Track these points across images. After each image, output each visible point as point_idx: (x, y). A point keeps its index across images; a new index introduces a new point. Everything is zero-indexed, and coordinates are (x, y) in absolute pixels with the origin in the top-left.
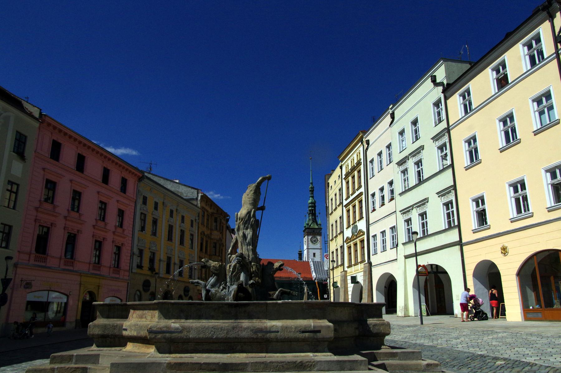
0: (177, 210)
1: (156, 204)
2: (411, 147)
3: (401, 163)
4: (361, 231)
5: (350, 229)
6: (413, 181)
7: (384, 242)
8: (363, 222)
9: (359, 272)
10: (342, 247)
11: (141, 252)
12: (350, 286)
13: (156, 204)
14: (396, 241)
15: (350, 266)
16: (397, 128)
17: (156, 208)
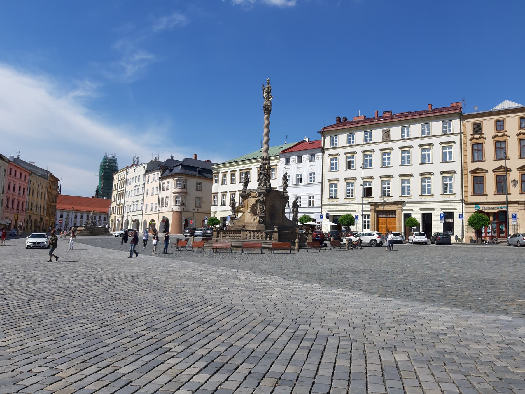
1: (34, 182)
2: (137, 184)
3: (135, 186)
4: (122, 203)
5: (119, 201)
8: (123, 200)
9: (119, 217)
10: (116, 207)
11: (28, 203)
12: (117, 222)
13: (34, 182)
15: (117, 215)
17: (34, 185)
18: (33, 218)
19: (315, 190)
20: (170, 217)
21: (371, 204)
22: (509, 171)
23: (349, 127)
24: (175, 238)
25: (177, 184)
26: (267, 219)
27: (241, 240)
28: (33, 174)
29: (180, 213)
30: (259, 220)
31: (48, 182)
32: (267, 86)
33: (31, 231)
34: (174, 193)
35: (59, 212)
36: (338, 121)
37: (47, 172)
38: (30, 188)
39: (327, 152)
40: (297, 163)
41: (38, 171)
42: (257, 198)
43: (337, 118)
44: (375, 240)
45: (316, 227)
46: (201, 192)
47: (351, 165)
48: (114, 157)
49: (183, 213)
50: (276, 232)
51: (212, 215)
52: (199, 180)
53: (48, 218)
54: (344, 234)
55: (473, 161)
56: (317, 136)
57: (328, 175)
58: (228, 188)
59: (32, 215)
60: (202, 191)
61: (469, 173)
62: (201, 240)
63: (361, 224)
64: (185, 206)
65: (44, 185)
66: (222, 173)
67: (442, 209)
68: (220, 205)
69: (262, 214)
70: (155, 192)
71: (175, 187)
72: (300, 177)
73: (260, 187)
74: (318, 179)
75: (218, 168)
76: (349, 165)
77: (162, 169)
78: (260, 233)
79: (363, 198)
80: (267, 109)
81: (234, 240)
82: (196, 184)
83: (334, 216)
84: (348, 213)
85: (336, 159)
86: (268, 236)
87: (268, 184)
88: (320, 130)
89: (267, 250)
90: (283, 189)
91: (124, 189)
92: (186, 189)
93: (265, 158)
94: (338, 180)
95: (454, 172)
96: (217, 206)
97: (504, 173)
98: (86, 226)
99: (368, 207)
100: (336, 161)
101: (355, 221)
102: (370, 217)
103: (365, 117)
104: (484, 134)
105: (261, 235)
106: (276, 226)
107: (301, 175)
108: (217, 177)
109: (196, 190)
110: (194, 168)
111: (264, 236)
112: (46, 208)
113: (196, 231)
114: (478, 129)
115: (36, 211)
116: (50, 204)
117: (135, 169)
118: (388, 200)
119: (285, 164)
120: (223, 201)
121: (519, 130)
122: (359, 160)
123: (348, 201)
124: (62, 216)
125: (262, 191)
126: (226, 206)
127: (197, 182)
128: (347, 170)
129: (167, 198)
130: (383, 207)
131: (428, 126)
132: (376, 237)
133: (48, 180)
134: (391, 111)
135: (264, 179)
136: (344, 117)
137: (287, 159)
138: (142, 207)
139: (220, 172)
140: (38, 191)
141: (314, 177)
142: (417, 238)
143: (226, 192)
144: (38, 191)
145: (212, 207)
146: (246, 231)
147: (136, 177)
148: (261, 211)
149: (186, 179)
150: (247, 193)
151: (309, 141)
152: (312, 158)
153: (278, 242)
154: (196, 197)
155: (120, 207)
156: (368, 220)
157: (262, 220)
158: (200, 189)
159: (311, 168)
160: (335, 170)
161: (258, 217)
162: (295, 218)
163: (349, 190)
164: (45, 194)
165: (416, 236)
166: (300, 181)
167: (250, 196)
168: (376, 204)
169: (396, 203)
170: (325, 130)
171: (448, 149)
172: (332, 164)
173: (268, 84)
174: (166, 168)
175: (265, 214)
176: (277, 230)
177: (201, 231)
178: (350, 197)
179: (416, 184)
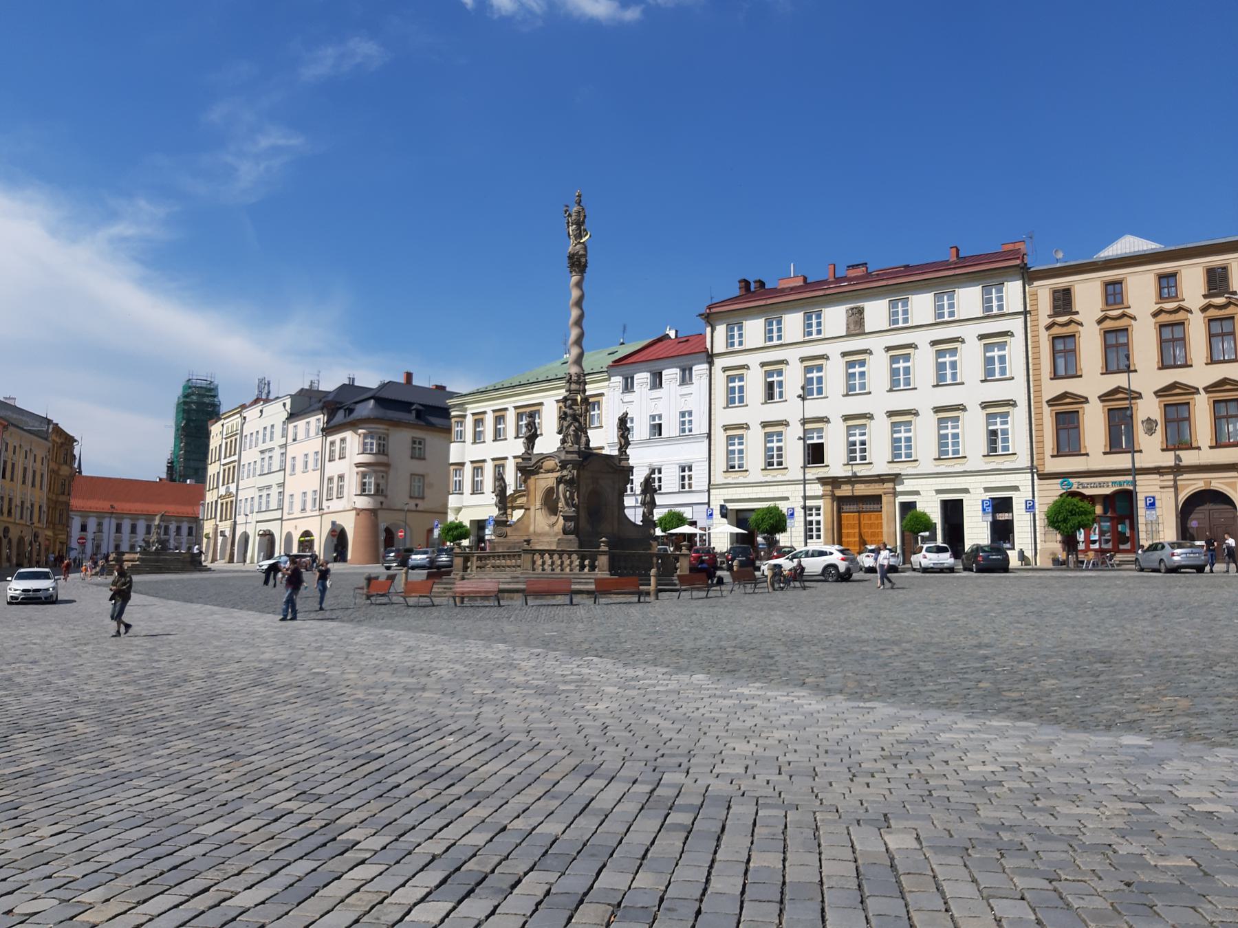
0: (31, 450)
1: (15, 447)
2: (268, 445)
3: (262, 452)
4: (231, 493)
8: (235, 484)
10: (216, 501)
12: (220, 539)
13: (15, 447)
15: (221, 521)
17: (14, 453)
18: (14, 534)
19: (695, 452)
20: (349, 524)
21: (823, 481)
22: (1135, 398)
23: (770, 301)
24: (362, 574)
25: (365, 444)
26: (583, 523)
27: (522, 574)
28: (11, 428)
29: (373, 512)
30: (565, 525)
31: (50, 445)
32: (576, 208)
33: (10, 566)
34: (358, 465)
35: (79, 518)
36: (743, 289)
37: (46, 421)
38: (5, 462)
39: (719, 363)
40: (651, 389)
41: (24, 418)
42: (558, 474)
43: (740, 282)
44: (834, 566)
45: (698, 539)
46: (423, 461)
47: (777, 390)
48: (211, 382)
49: (380, 513)
50: (604, 553)
51: (451, 517)
52: (419, 434)
53: (50, 533)
54: (762, 553)
55: (1055, 377)
56: (695, 325)
57: (724, 416)
58: (488, 450)
60: (424, 459)
61: (1045, 406)
62: (425, 577)
63: (802, 529)
64: (386, 496)
65: (41, 453)
66: (473, 414)
67: (987, 490)
68: (470, 492)
69: (571, 512)
70: (311, 465)
71: (361, 451)
72: (657, 422)
73: (564, 448)
74: (700, 426)
75: (462, 404)
76: (771, 391)
77: (328, 409)
78: (565, 556)
79: (804, 467)
80: (578, 263)
81: (504, 576)
82: (410, 441)
83: (738, 511)
84: (771, 504)
85: (741, 378)
86: (586, 562)
87: (583, 439)
88: (703, 310)
89: (585, 596)
90: (619, 449)
91: (236, 458)
92: (387, 455)
93: (574, 378)
94: (746, 427)
95: (1011, 403)
96: (462, 494)
97: (1125, 404)
98: (145, 549)
99: (816, 489)
100: (741, 384)
101: (788, 521)
102: (822, 512)
103: (805, 279)
104: (1077, 313)
105: (568, 562)
106: (604, 539)
107: (660, 417)
108: (461, 426)
109: (412, 458)
110: (405, 406)
111: (577, 563)
112: (45, 508)
113: (414, 557)
114: (1063, 301)
115: (21, 518)
116: (54, 498)
117: (261, 411)
118: (862, 471)
119: (623, 393)
120: (477, 481)
121: (1156, 303)
122: (793, 378)
123: (771, 476)
124: (84, 528)
125: (570, 457)
126: (483, 493)
127: (413, 438)
128: (766, 403)
129: (341, 477)
130: (851, 488)
131: (951, 298)
132: (836, 558)
133: (49, 441)
134: (866, 264)
135: (572, 428)
136: (758, 279)
137: (626, 379)
138: (281, 501)
139: (469, 413)
140: (25, 469)
141: (690, 421)
142: (930, 560)
143: (484, 461)
144: (25, 469)
145: (451, 497)
146: (534, 552)
147: (265, 428)
148: (567, 504)
149: (386, 431)
150: (533, 461)
151: (676, 336)
152: (686, 379)
153: (609, 577)
154: (412, 475)
155: (227, 503)
156: (818, 518)
157: (571, 525)
158: (420, 454)
159: (683, 400)
160: (739, 403)
161: (561, 518)
162: (648, 521)
163: (771, 449)
164: (42, 475)
165: (928, 555)
166: (657, 431)
167: (541, 468)
168: (834, 482)
169: (880, 479)
170: (713, 310)
171: (996, 349)
172: (731, 391)
173: (579, 205)
174: (338, 405)
175: (577, 512)
176: (606, 549)
177: (424, 556)
178: (775, 467)
179: (925, 433)
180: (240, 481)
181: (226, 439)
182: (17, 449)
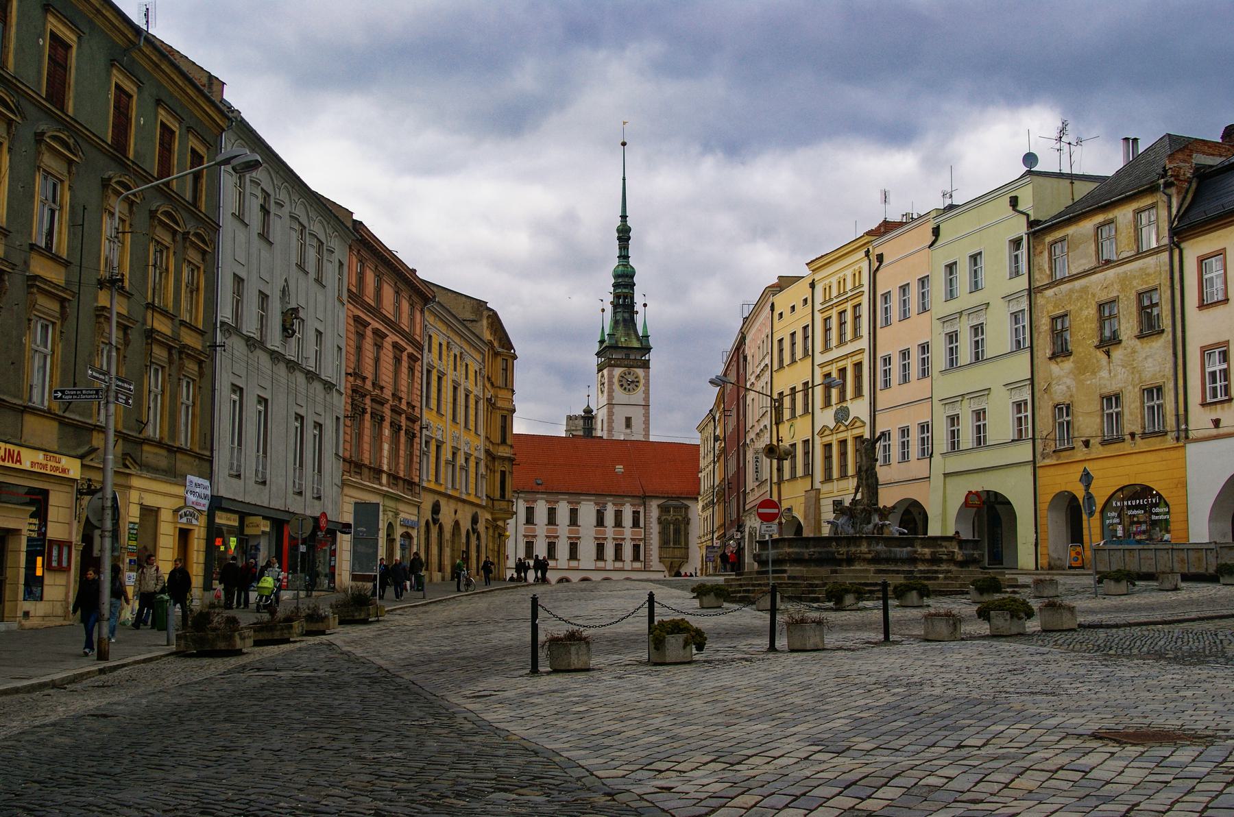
1: (440, 345)
2: (965, 299)
3: (944, 320)
6: (965, 353)
7: (904, 445)
13: (440, 345)
14: (928, 448)
16: (942, 256)
59: (443, 502)
112: (482, 470)
117: (936, 232)
147: (904, 289)
155: (843, 443)
180: (879, 395)
181: (822, 311)
182: (444, 347)
